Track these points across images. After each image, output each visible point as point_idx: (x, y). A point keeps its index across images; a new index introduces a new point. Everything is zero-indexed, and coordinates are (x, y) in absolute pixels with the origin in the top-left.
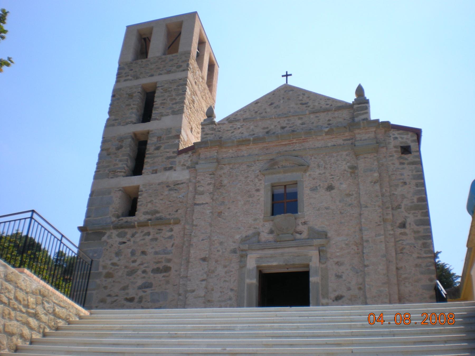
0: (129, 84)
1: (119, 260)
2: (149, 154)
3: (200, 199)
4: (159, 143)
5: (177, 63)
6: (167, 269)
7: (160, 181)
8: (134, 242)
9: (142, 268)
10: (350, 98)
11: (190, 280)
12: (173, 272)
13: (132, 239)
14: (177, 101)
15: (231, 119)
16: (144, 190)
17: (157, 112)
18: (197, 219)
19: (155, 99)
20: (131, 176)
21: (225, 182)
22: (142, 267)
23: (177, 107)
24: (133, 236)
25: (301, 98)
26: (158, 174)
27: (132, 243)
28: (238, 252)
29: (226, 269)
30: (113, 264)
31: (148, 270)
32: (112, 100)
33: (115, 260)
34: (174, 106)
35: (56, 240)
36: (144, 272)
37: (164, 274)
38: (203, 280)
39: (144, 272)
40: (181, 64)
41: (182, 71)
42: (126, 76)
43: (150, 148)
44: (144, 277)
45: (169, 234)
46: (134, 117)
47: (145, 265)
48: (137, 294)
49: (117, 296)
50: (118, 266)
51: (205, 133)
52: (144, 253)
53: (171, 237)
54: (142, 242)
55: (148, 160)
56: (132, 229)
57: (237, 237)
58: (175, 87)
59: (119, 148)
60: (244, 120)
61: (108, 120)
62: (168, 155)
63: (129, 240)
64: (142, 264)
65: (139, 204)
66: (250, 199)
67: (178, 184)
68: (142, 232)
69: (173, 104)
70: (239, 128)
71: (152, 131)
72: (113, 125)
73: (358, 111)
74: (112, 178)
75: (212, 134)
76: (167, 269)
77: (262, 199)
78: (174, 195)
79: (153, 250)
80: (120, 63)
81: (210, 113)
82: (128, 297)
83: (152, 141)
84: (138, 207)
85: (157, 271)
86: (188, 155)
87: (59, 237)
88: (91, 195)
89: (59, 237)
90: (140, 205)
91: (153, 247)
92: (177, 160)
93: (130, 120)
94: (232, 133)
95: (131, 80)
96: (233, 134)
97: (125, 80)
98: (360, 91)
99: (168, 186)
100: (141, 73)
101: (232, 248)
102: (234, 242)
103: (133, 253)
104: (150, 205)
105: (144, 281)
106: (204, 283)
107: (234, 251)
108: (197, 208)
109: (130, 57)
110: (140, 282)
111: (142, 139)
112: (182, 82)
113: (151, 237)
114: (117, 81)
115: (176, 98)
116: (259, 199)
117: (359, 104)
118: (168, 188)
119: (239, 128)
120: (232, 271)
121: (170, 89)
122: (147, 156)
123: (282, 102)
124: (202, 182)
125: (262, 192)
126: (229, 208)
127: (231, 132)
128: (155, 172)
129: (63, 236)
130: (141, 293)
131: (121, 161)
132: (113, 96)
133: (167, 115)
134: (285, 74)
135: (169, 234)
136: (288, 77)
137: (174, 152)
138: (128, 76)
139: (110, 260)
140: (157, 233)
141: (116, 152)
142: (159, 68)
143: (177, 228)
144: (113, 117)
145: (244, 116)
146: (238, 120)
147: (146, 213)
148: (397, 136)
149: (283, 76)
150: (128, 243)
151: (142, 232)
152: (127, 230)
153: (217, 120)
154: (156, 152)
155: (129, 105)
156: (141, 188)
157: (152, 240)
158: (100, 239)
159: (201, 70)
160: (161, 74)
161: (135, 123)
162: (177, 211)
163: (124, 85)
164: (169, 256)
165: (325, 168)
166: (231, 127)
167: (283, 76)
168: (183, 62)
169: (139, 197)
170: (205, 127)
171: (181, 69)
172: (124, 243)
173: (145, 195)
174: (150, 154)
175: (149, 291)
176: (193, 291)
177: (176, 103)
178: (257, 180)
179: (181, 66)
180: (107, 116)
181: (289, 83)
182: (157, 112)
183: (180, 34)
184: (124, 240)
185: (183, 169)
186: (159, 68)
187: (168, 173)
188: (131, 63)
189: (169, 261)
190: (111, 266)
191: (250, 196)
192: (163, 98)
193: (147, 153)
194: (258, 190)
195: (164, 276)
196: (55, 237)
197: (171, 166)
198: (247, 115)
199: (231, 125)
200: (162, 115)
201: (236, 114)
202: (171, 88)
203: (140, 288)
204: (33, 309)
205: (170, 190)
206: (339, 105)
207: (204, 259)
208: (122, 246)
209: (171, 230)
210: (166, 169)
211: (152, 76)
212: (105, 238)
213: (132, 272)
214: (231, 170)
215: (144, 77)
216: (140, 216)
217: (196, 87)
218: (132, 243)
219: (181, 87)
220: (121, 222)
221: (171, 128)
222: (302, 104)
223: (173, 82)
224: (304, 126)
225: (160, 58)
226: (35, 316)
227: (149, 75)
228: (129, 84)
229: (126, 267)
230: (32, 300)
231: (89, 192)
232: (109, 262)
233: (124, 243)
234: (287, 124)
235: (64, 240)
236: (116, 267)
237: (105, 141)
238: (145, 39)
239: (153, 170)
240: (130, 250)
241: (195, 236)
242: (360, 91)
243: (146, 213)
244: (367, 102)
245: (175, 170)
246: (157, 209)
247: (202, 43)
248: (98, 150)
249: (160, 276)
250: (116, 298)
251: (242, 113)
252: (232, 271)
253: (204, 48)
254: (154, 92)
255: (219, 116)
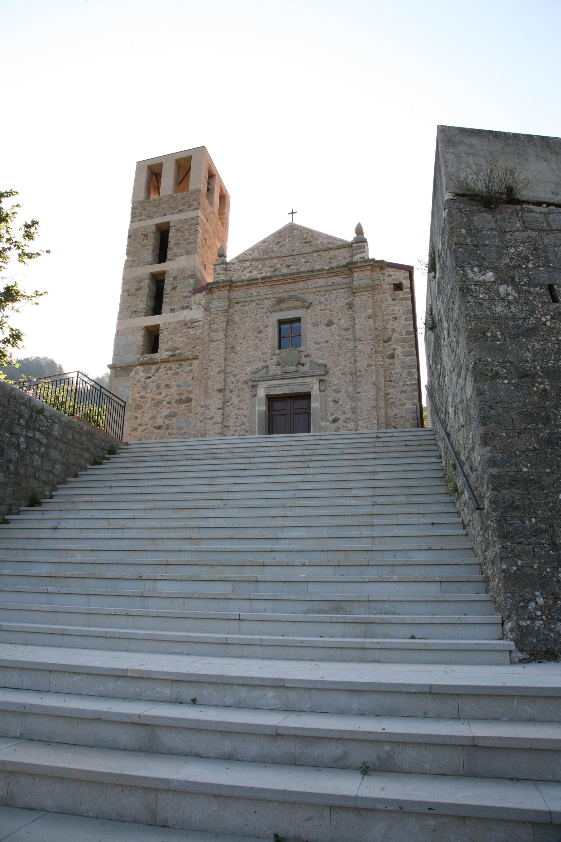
0: (143, 224)
1: (146, 393)
2: (167, 294)
3: (214, 336)
4: (176, 283)
5: (188, 202)
6: (189, 400)
7: (179, 320)
8: (158, 376)
9: (167, 399)
10: (349, 236)
11: (209, 409)
12: (193, 403)
13: (156, 374)
14: (190, 241)
15: (241, 259)
16: (164, 328)
17: (172, 252)
18: (212, 354)
19: (169, 240)
20: (152, 315)
21: (237, 319)
22: (166, 398)
23: (190, 247)
24: (157, 371)
25: (305, 236)
26: (176, 313)
27: (156, 377)
28: (249, 383)
29: (240, 398)
30: (142, 397)
31: (172, 401)
32: (129, 242)
33: (143, 393)
34: (187, 246)
35: (97, 391)
36: (168, 403)
37: (187, 404)
38: (220, 409)
39: (168, 403)
40: (192, 202)
41: (193, 210)
42: (140, 216)
43: (167, 288)
44: (169, 408)
45: (189, 368)
46: (150, 258)
47: (169, 397)
48: (164, 423)
49: (146, 425)
50: (146, 398)
51: (216, 273)
52: (167, 386)
53: (190, 371)
54: (165, 376)
55: (166, 300)
56: (155, 365)
57: (249, 369)
58: (188, 227)
59: (138, 290)
60: (254, 260)
61: (127, 261)
62: (184, 294)
63: (154, 375)
64: (166, 396)
65: (160, 341)
66: (260, 335)
67: (194, 322)
68: (165, 367)
69: (186, 244)
70: (248, 267)
71: (168, 271)
72: (132, 266)
73: (356, 249)
74: (134, 318)
75: (224, 274)
76: (189, 400)
77: (270, 335)
78: (192, 332)
79: (176, 383)
80: (134, 203)
81: (222, 255)
82: (157, 425)
83: (168, 282)
84: (160, 345)
85: (180, 401)
86: (203, 294)
87: (99, 388)
88: (117, 335)
89: (99, 388)
90: (161, 343)
91: (176, 381)
92: (193, 298)
93: (146, 261)
94: (243, 271)
95: (145, 220)
96: (243, 273)
97: (140, 220)
98: (359, 230)
99: (186, 324)
100: (155, 213)
101: (244, 379)
102: (246, 374)
103: (158, 387)
104: (170, 342)
105: (169, 411)
106: (221, 411)
107: (246, 382)
108: (212, 345)
109: (142, 196)
110: (166, 412)
111: (160, 278)
112: (194, 221)
113: (173, 372)
114: (132, 221)
115: (189, 238)
116: (267, 335)
117: (357, 243)
118: (186, 326)
119: (248, 267)
120: (244, 400)
121: (182, 229)
122: (165, 296)
123: (287, 240)
124: (216, 320)
125: (270, 329)
126: (241, 344)
127: (241, 271)
128: (173, 310)
129: (101, 387)
130: (167, 422)
131: (141, 301)
132: (129, 237)
133: (181, 256)
134: (291, 212)
135: (189, 368)
136: (294, 214)
137: (189, 292)
138: (142, 215)
139: (139, 393)
140: (178, 368)
141: (136, 292)
142: (171, 207)
143: (195, 363)
144: (130, 258)
145: (253, 256)
146: (247, 260)
147: (167, 350)
148: (390, 273)
149: (289, 214)
150: (153, 378)
151: (165, 367)
152: (151, 366)
153: (228, 259)
154: (173, 292)
155: (145, 246)
156: (161, 326)
157: (174, 374)
158: (128, 375)
159: (211, 204)
160: (174, 213)
161: (152, 264)
162: (195, 347)
163: (138, 225)
164: (190, 389)
165: (325, 304)
166: (241, 266)
167: (289, 214)
168: (194, 201)
169: (160, 335)
170: (216, 267)
171: (193, 208)
172: (150, 377)
173: (165, 333)
174: (167, 294)
175: (174, 420)
176: (212, 418)
177: (189, 243)
178: (265, 318)
179: (192, 205)
180: (125, 258)
181: (295, 222)
182: (172, 252)
183: (190, 169)
184: (150, 375)
185: (199, 308)
186: (171, 207)
187: (185, 312)
188: (144, 202)
189: (190, 392)
190: (140, 399)
191: (260, 332)
192: (177, 238)
193: (164, 293)
194: (266, 326)
195: (186, 406)
196: (96, 389)
197: (187, 305)
198: (256, 255)
199: (241, 265)
200: (176, 255)
201: (244, 254)
202: (183, 227)
203: (166, 417)
204: (86, 445)
205: (189, 328)
206: (340, 243)
207: (220, 391)
208: (148, 380)
209: (191, 365)
210: (183, 308)
211: (165, 215)
212: (132, 373)
213: (158, 404)
214: (242, 308)
215: (158, 217)
216: (163, 353)
217: (208, 225)
218: (156, 377)
219: (193, 227)
220: (145, 359)
221: (186, 269)
222: (306, 243)
223: (185, 221)
224: (307, 264)
225: (171, 197)
226: (87, 450)
227: (162, 214)
228: (143, 224)
229: (153, 399)
230: (84, 439)
231: (114, 332)
232: (138, 396)
233: (150, 377)
234: (292, 262)
235: (103, 390)
236: (144, 400)
237: (125, 282)
238: (156, 174)
239: (171, 309)
240: (155, 384)
241: (211, 370)
242: (359, 230)
243: (167, 350)
244: (365, 241)
245: (191, 309)
246: (176, 345)
247: (212, 175)
248: (120, 291)
249: (183, 406)
250: (146, 427)
251: (251, 252)
252: (244, 400)
253: (215, 182)
254: (168, 232)
255: (231, 255)
